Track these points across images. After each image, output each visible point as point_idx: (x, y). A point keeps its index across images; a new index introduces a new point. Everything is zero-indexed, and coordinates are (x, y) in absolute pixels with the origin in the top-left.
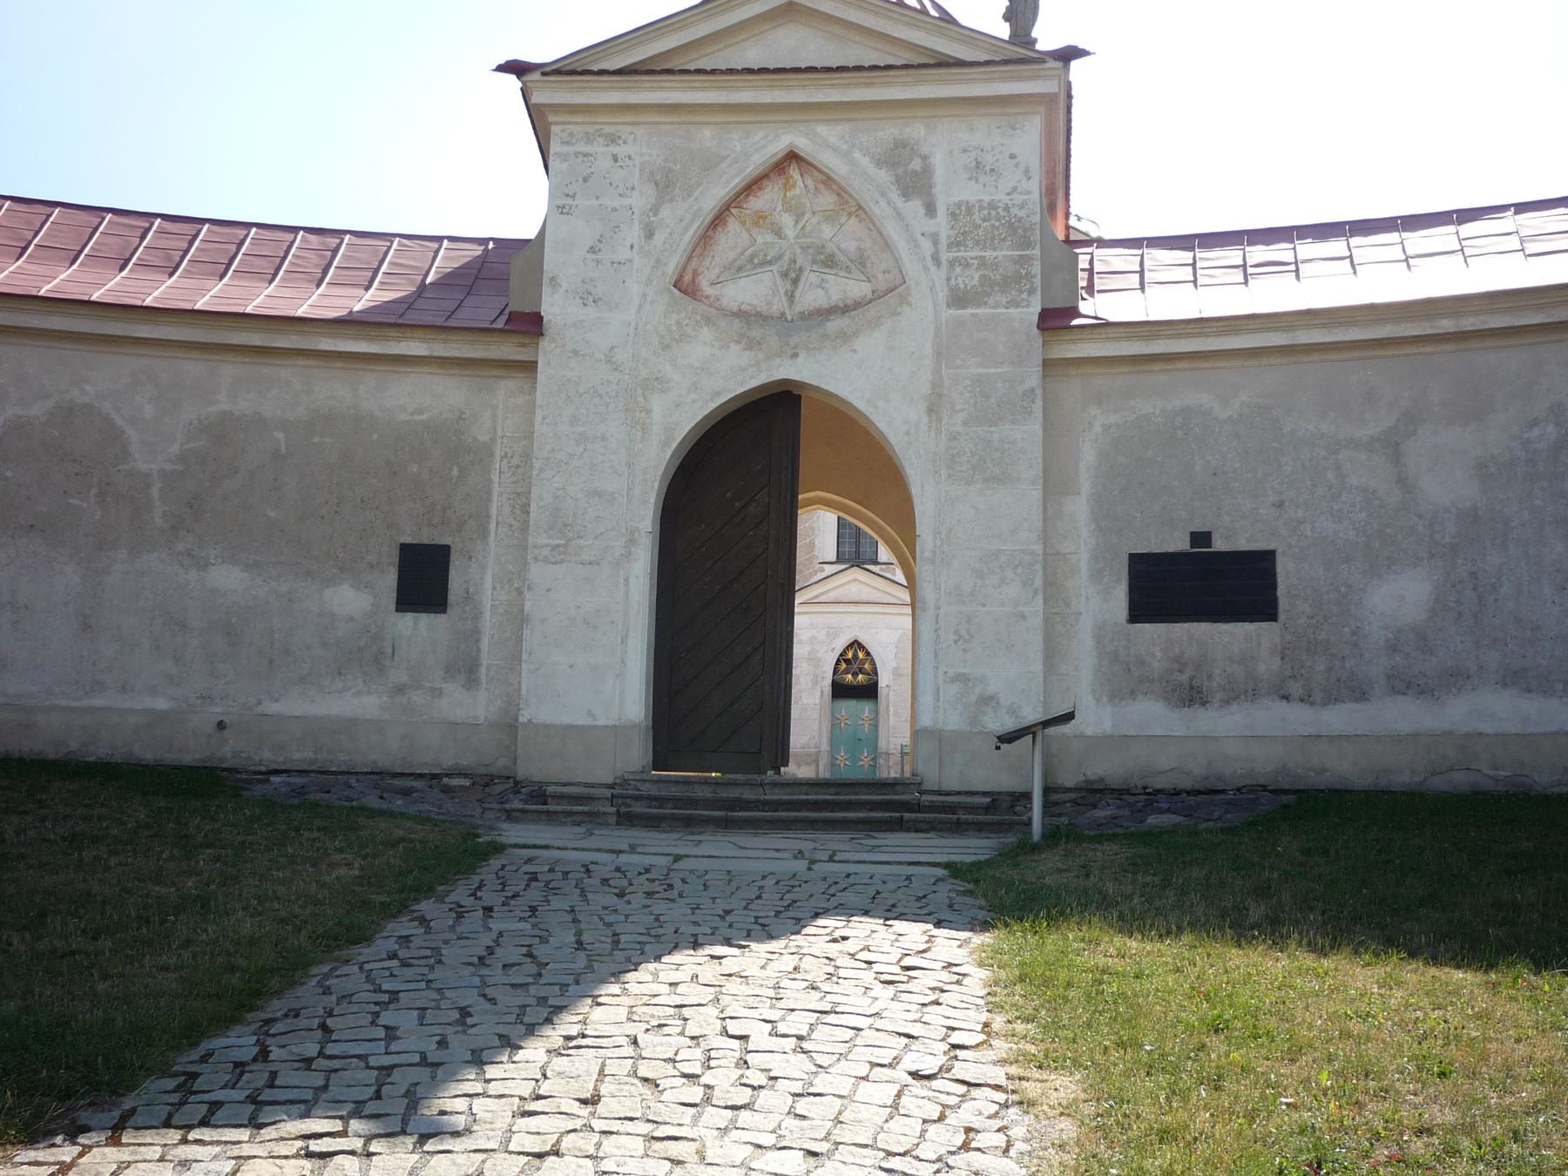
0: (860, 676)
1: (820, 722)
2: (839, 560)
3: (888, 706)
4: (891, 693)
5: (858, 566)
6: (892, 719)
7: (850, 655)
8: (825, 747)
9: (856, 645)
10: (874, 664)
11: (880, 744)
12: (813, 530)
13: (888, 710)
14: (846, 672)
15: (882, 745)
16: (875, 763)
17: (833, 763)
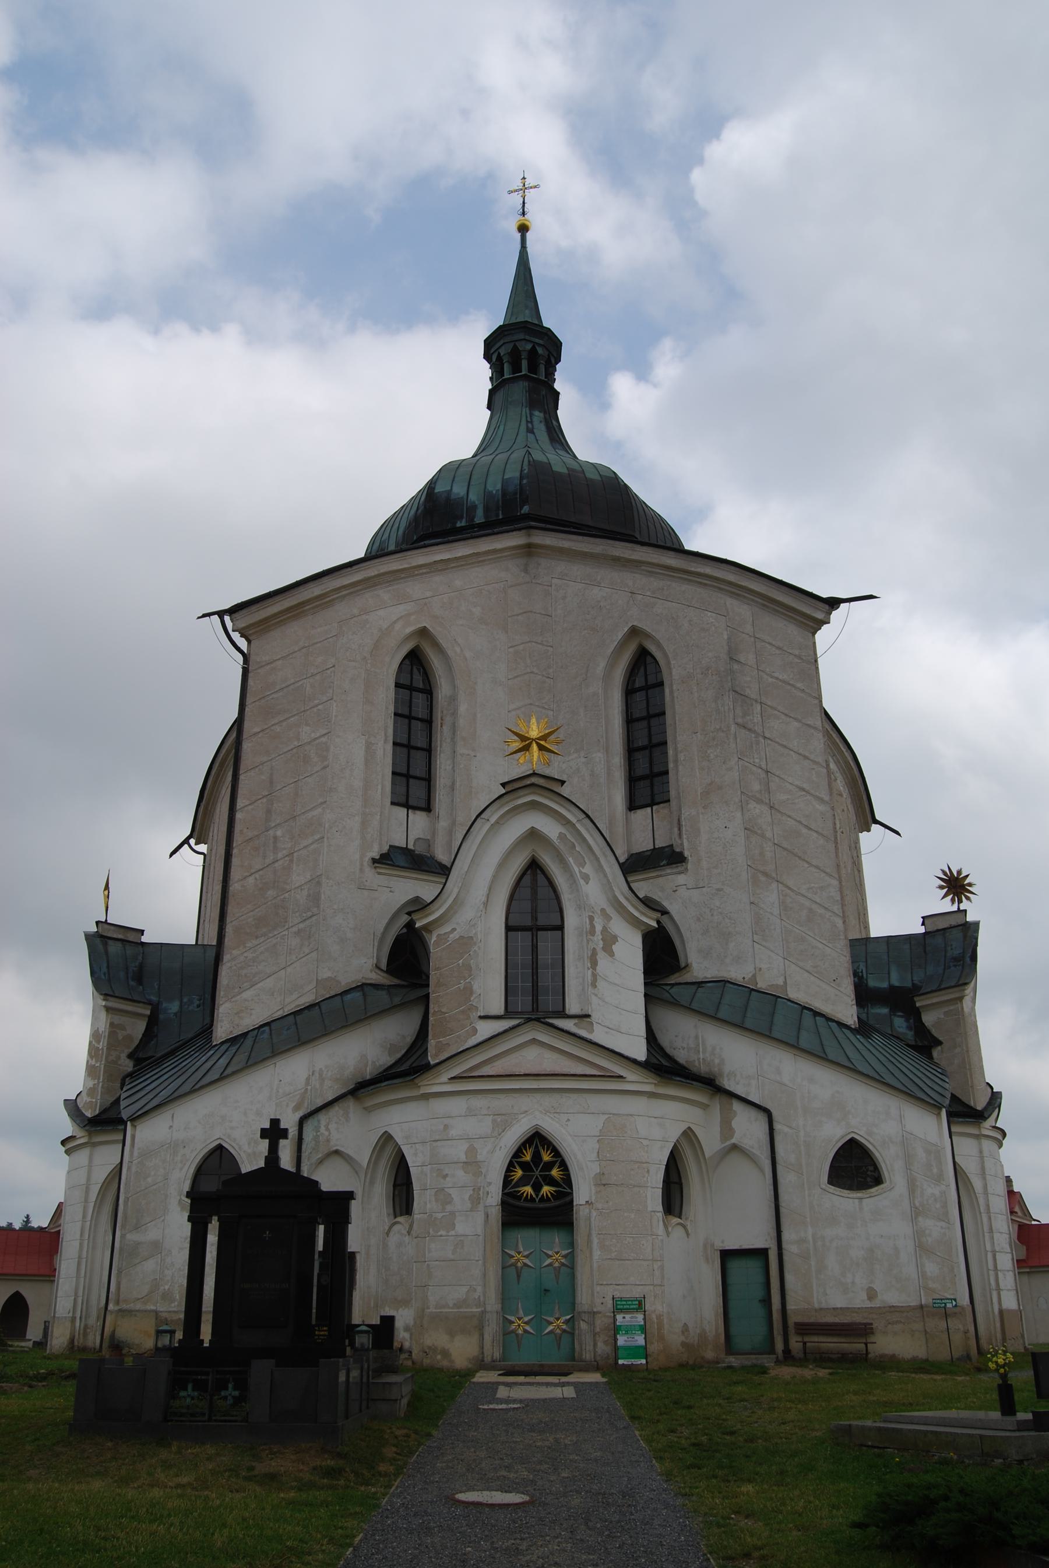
0: (546, 1189)
1: (484, 1263)
2: (509, 1013)
3: (589, 1235)
4: (594, 1213)
5: (538, 1020)
6: (597, 1254)
7: (528, 1157)
8: (493, 1304)
9: (537, 1139)
11: (578, 1300)
12: (469, 968)
13: (589, 1241)
14: (522, 1181)
15: (583, 1299)
16: (573, 1328)
17: (507, 1332)
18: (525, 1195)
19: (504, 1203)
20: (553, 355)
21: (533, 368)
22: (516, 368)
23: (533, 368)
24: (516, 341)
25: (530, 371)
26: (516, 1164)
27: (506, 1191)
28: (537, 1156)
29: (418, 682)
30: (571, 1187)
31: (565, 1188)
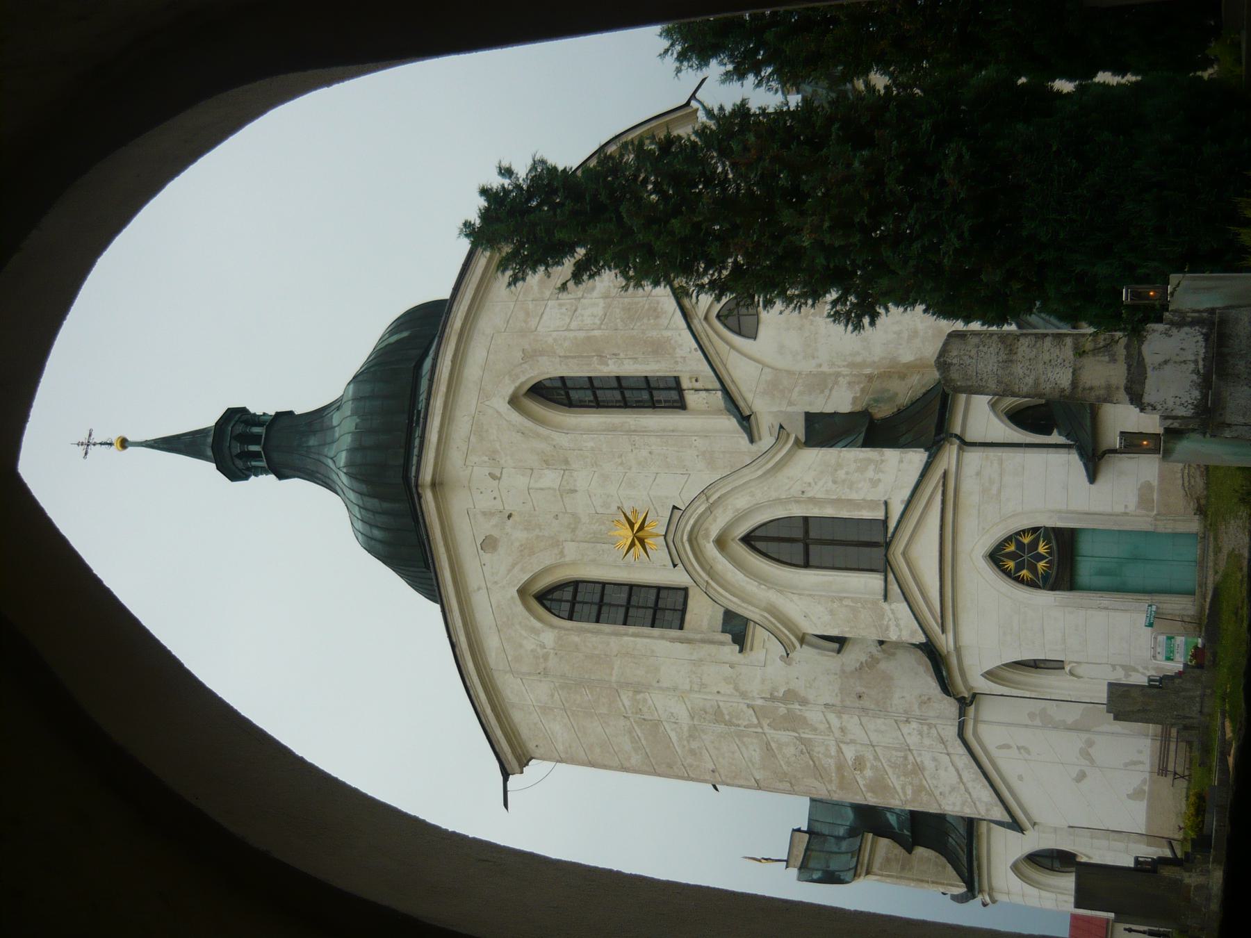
0: (1042, 549)
7: (1011, 564)
9: (996, 557)
10: (1024, 531)
14: (1033, 569)
18: (1044, 568)
19: (1053, 589)
20: (239, 418)
21: (256, 439)
22: (256, 455)
23: (256, 439)
24: (231, 455)
25: (259, 444)
26: (1017, 575)
27: (1041, 585)
28: (1011, 556)
29: (568, 594)
30: (1041, 527)
31: (1040, 533)
